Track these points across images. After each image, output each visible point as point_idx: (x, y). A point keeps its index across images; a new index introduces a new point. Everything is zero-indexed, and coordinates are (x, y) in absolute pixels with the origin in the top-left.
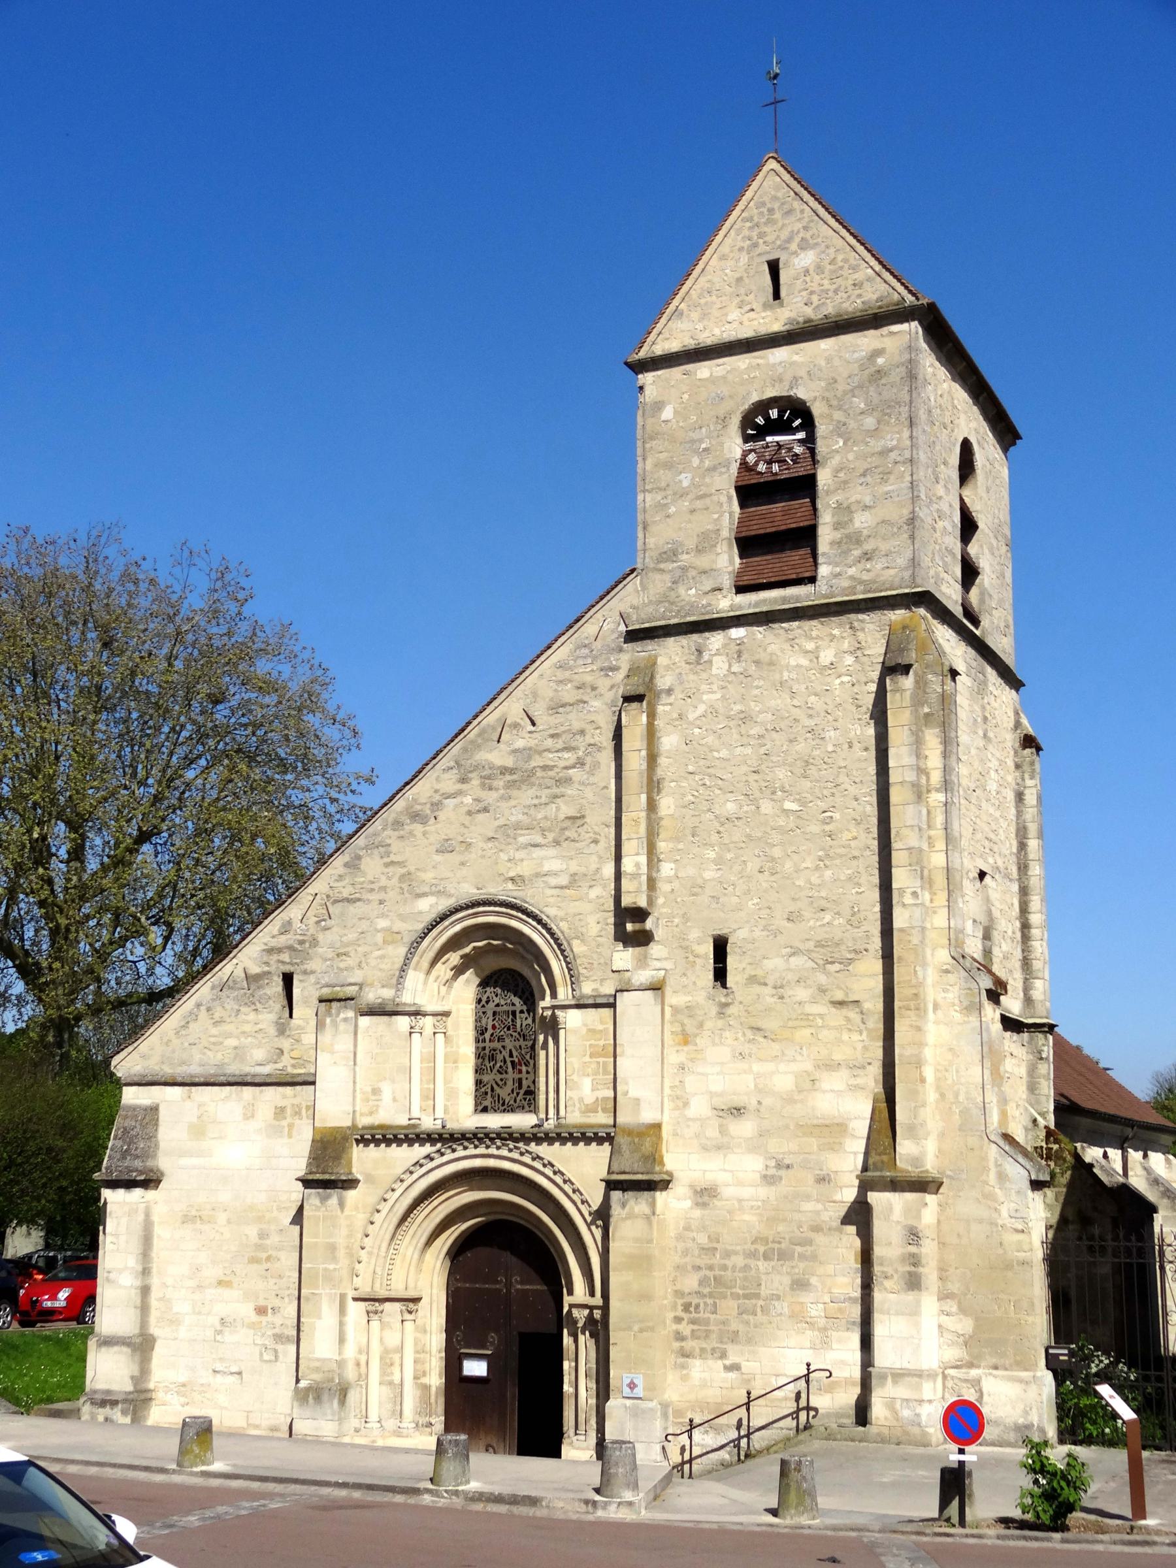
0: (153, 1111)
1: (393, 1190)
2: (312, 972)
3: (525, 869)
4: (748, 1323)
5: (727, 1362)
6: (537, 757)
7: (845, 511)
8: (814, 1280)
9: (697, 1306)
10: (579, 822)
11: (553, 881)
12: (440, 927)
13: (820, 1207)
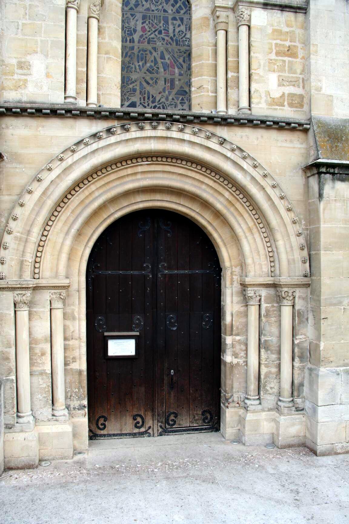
1: (50, 170)
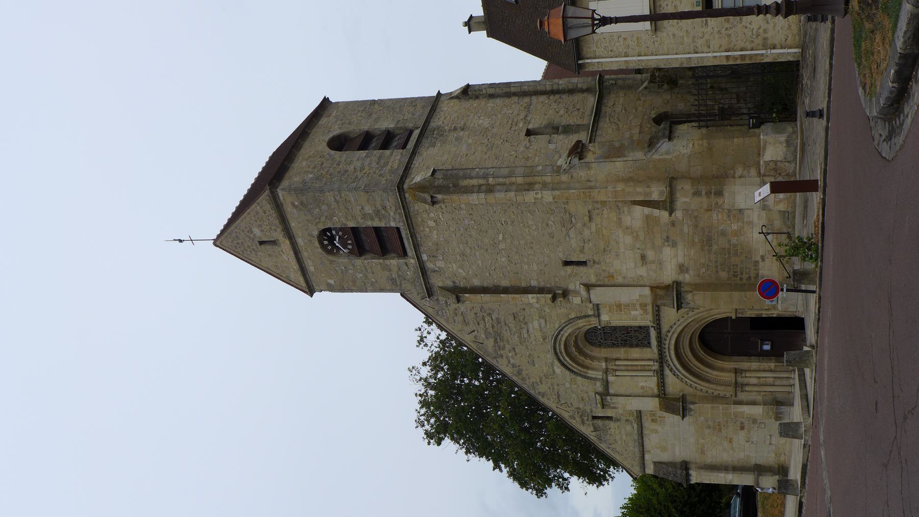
0: (656, 464)
2: (591, 409)
3: (539, 335)
4: (742, 253)
5: (760, 260)
6: (488, 330)
7: (365, 216)
8: (721, 228)
9: (734, 272)
10: (516, 315)
11: (543, 325)
12: (568, 365)
13: (686, 226)
